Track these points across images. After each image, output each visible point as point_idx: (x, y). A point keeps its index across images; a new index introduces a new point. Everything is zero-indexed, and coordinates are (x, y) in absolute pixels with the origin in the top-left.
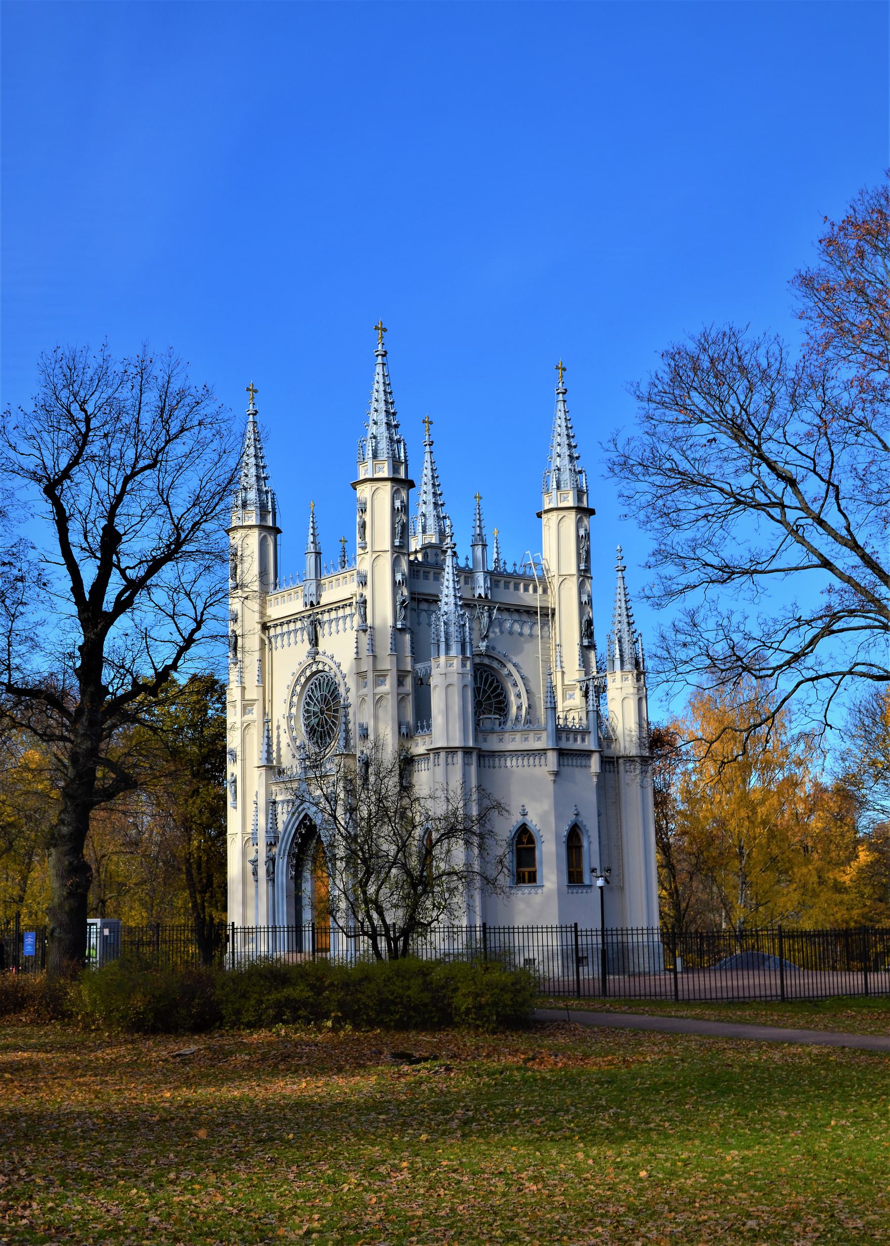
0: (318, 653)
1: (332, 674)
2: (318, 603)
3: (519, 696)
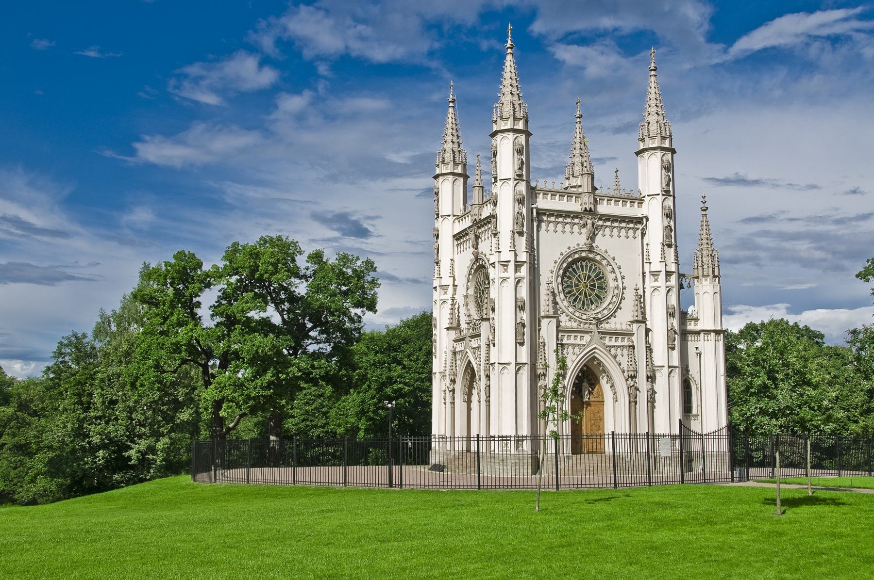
3: (616, 279)
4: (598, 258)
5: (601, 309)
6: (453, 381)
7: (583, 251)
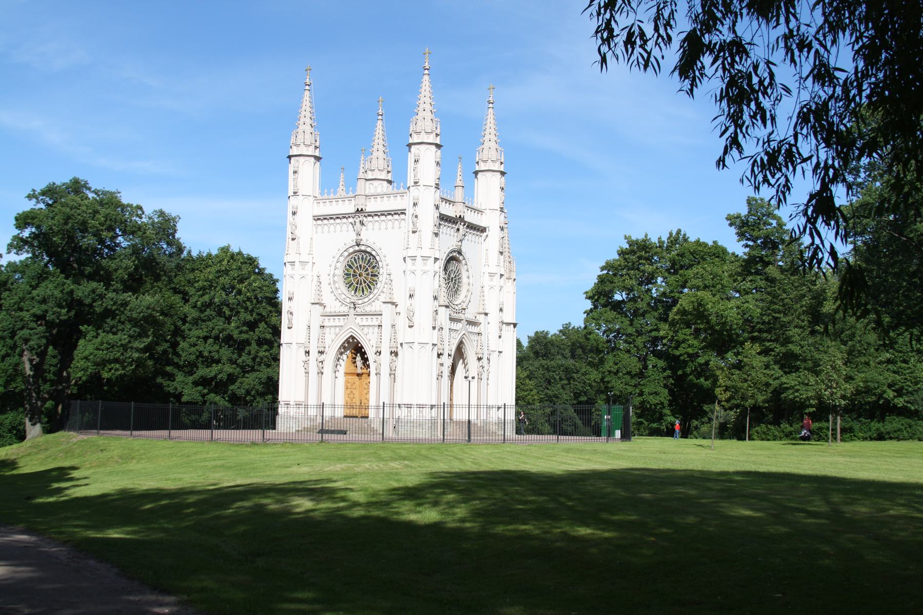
4: (461, 258)
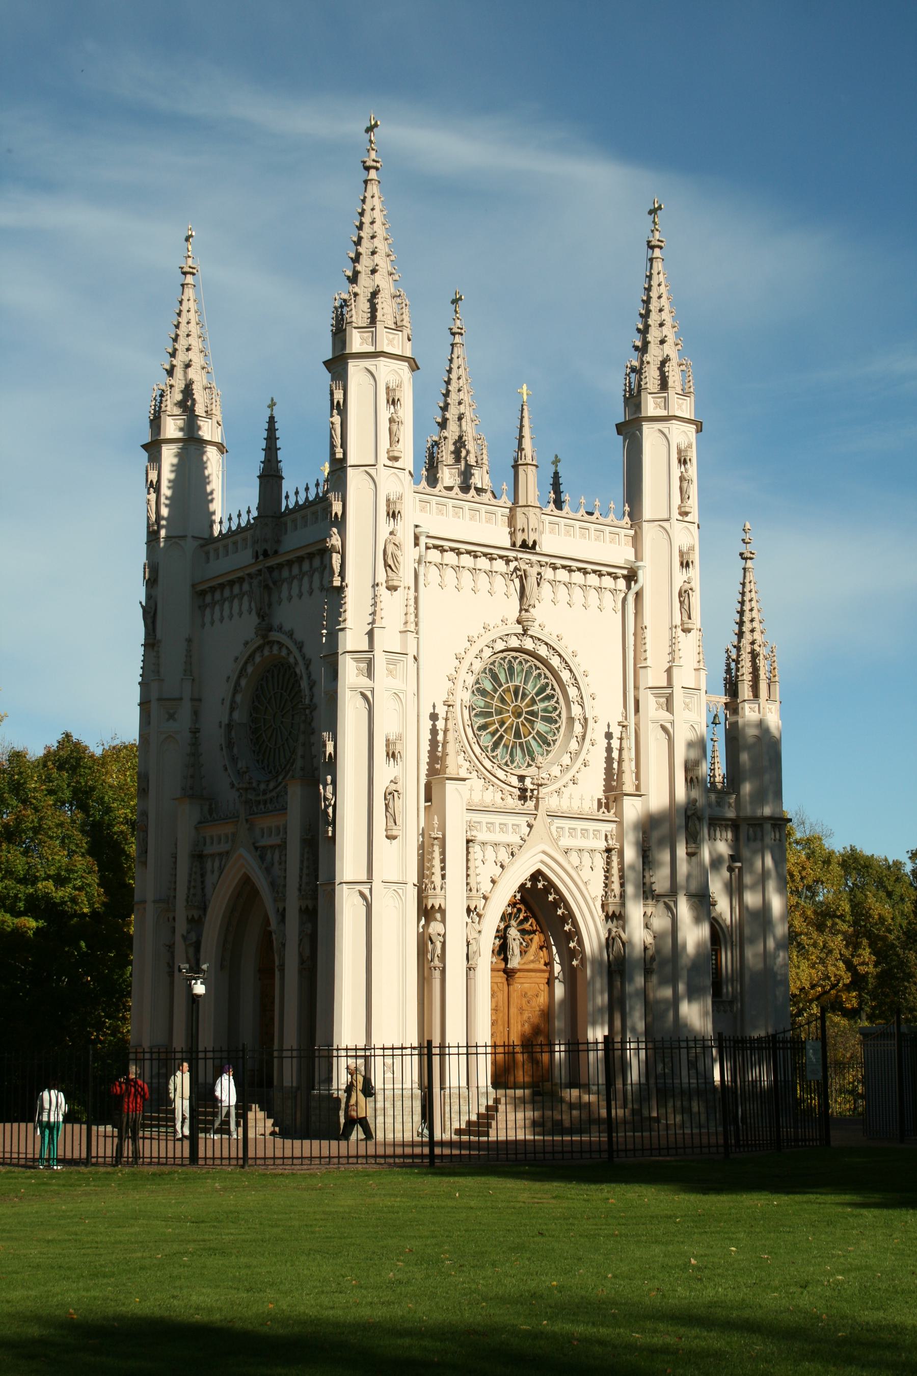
0: (270, 629)
1: (292, 660)
2: (276, 552)
5: (549, 766)
6: (196, 923)
7: (515, 635)
